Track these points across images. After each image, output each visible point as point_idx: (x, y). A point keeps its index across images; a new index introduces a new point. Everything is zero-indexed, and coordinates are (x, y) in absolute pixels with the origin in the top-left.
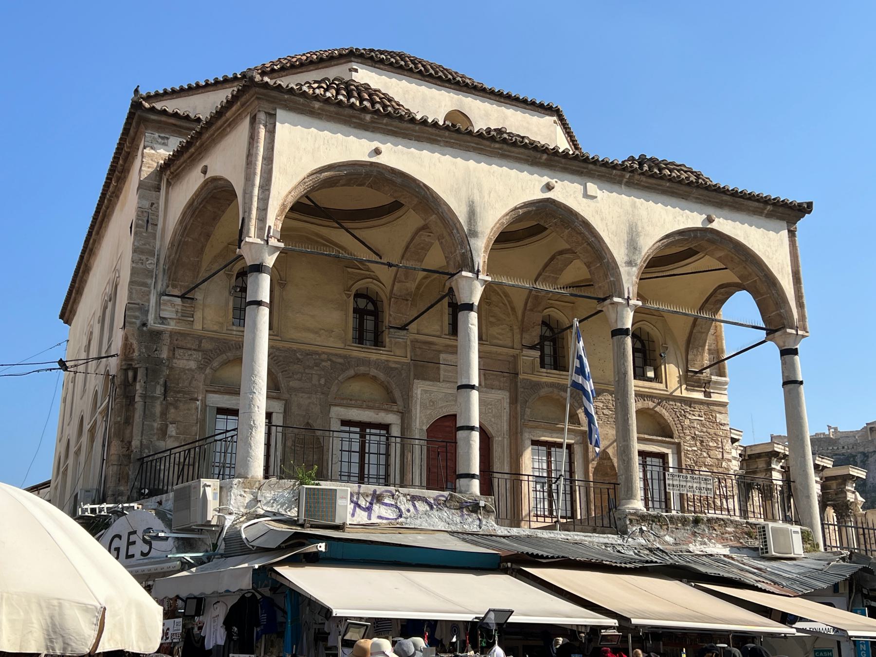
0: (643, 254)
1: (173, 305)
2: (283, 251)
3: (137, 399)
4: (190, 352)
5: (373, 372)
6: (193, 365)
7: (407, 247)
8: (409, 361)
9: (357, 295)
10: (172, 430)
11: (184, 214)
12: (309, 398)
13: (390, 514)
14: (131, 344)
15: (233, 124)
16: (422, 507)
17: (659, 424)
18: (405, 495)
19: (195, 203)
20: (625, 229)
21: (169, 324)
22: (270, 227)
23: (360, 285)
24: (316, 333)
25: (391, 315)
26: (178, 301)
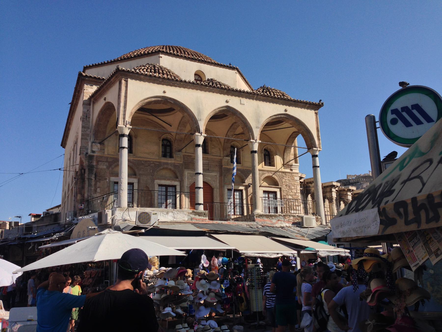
0: (261, 124)
2: (132, 129)
3: (86, 180)
4: (104, 163)
5: (170, 167)
6: (105, 167)
7: (180, 123)
8: (182, 163)
9: (163, 140)
10: (98, 190)
11: (99, 114)
12: (147, 177)
14: (83, 161)
15: (113, 83)
17: (274, 181)
21: (96, 153)
22: (127, 121)
23: (164, 136)
24: (149, 154)
25: (175, 146)
26: (99, 145)
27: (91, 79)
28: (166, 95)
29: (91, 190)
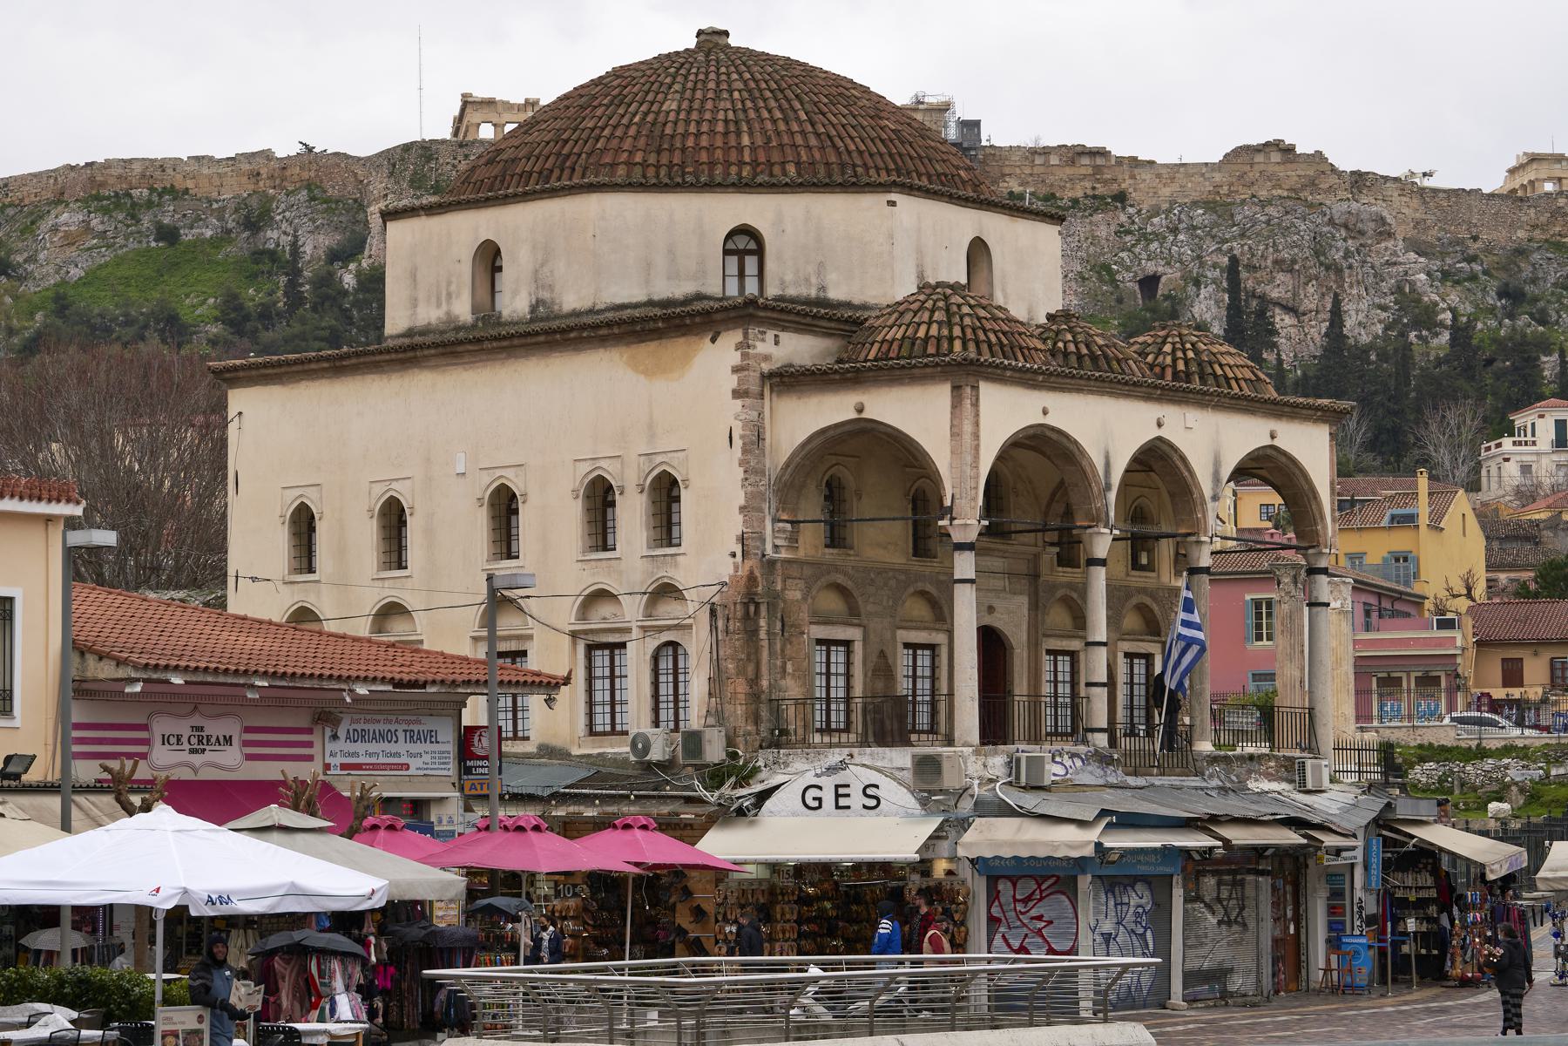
3: (763, 635)
6: (798, 595)
13: (1059, 770)
16: (1079, 763)
24: (885, 548)
26: (788, 526)
27: (769, 314)
28: (1051, 420)
29: (775, 665)
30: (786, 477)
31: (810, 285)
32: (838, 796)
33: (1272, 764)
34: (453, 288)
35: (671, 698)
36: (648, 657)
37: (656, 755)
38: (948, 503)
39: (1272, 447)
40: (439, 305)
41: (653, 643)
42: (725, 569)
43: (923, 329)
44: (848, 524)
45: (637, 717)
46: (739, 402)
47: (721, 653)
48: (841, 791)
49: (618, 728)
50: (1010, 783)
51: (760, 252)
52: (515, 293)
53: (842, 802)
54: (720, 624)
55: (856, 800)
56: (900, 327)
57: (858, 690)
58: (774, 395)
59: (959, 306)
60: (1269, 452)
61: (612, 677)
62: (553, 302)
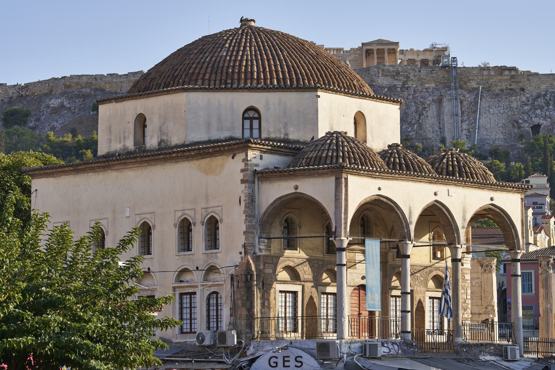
1: (264, 242)
4: (270, 265)
13: (386, 350)
18: (390, 342)
19: (284, 198)
20: (461, 210)
21: (262, 252)
24: (313, 250)
26: (266, 241)
30: (265, 218)
31: (281, 132)
32: (284, 361)
33: (492, 348)
34: (126, 134)
35: (215, 317)
36: (205, 299)
37: (207, 342)
38: (333, 230)
39: (492, 205)
40: (120, 142)
41: (207, 293)
42: (237, 259)
43: (325, 152)
44: (295, 239)
45: (200, 326)
46: (243, 185)
47: (235, 297)
48: (286, 359)
49: (193, 330)
50: (361, 356)
51: (259, 118)
52: (152, 137)
53: (286, 364)
54: (235, 284)
55: (292, 363)
56: (315, 151)
57: (300, 314)
58: (260, 182)
59: (342, 142)
60: (491, 206)
61: (191, 308)
62: (168, 141)
